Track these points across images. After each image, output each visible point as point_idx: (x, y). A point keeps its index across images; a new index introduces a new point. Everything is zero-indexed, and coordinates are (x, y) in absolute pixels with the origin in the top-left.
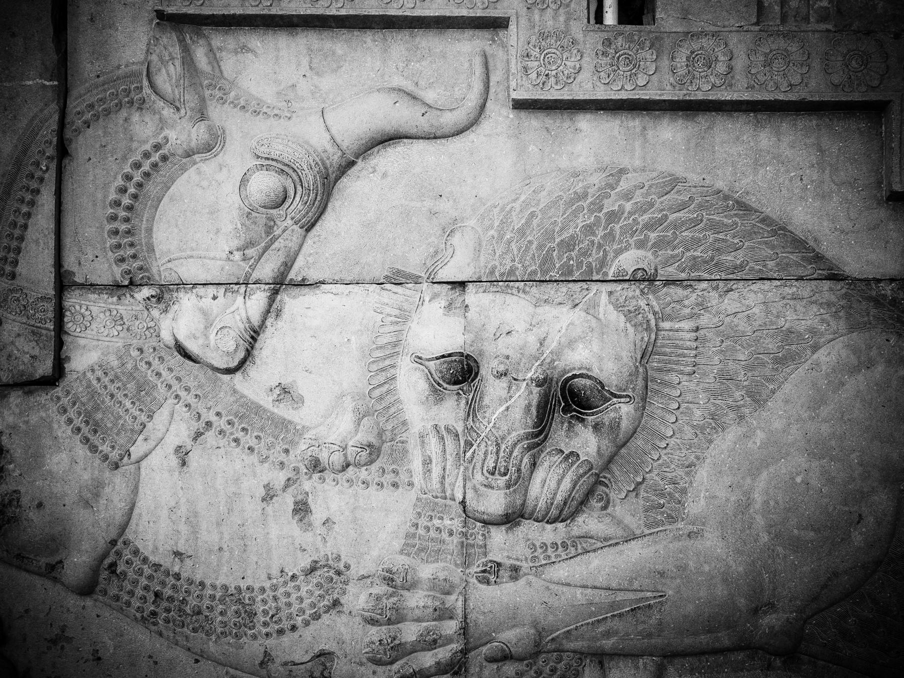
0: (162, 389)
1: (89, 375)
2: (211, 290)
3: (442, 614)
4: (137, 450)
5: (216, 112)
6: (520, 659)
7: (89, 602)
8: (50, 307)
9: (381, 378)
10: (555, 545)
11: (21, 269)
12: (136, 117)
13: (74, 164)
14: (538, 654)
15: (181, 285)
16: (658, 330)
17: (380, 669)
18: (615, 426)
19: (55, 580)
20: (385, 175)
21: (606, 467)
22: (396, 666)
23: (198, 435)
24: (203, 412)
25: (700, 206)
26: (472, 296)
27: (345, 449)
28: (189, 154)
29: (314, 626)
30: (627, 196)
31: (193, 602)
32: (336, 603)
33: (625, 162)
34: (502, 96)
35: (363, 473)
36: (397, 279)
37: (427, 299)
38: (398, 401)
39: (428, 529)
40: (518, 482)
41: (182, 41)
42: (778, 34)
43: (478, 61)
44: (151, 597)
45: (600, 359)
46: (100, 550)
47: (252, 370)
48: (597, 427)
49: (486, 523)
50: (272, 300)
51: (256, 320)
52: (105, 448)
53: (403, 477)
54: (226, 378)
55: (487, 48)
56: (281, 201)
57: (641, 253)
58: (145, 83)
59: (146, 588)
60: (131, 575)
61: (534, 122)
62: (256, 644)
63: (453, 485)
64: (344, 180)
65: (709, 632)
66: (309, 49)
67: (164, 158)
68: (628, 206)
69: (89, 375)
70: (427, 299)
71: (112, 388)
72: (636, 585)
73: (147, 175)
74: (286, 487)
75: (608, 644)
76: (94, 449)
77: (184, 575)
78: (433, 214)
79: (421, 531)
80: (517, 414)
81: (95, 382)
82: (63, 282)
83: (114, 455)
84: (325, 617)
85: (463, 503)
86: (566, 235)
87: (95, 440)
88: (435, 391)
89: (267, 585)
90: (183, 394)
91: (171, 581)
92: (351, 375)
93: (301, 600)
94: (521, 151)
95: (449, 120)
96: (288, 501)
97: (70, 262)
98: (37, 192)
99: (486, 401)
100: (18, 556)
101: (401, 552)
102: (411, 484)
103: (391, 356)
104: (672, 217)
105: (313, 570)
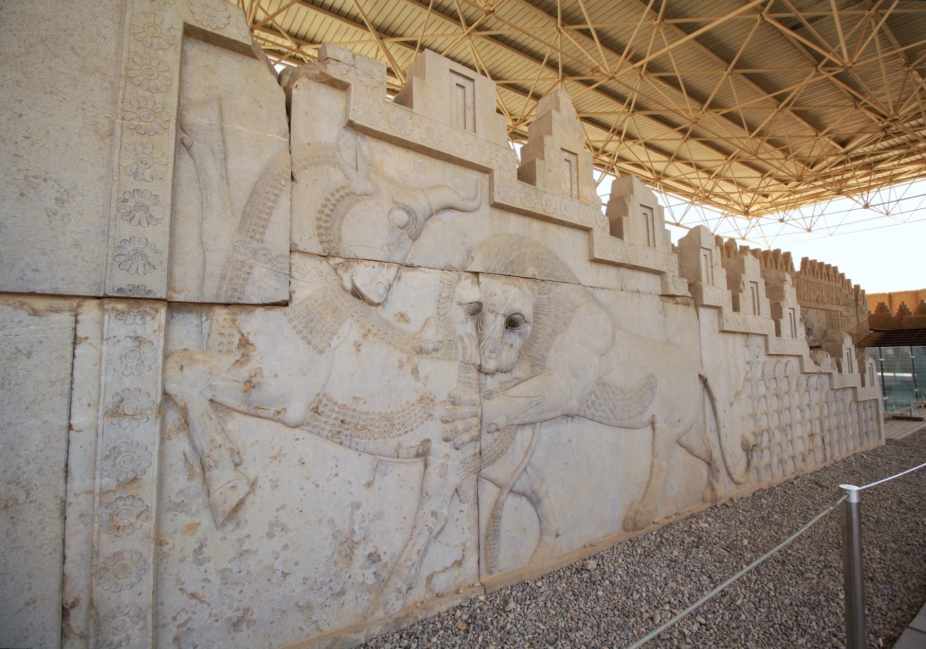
4: (334, 343)
11: (266, 238)
12: (332, 170)
15: (357, 260)
17: (447, 444)
19: (278, 421)
20: (444, 223)
23: (365, 335)
32: (431, 415)
48: (520, 335)
51: (391, 280)
59: (336, 419)
60: (327, 412)
76: (309, 343)
77: (358, 409)
81: (310, 306)
85: (480, 366)
96: (408, 368)
99: (487, 322)
105: (421, 400)
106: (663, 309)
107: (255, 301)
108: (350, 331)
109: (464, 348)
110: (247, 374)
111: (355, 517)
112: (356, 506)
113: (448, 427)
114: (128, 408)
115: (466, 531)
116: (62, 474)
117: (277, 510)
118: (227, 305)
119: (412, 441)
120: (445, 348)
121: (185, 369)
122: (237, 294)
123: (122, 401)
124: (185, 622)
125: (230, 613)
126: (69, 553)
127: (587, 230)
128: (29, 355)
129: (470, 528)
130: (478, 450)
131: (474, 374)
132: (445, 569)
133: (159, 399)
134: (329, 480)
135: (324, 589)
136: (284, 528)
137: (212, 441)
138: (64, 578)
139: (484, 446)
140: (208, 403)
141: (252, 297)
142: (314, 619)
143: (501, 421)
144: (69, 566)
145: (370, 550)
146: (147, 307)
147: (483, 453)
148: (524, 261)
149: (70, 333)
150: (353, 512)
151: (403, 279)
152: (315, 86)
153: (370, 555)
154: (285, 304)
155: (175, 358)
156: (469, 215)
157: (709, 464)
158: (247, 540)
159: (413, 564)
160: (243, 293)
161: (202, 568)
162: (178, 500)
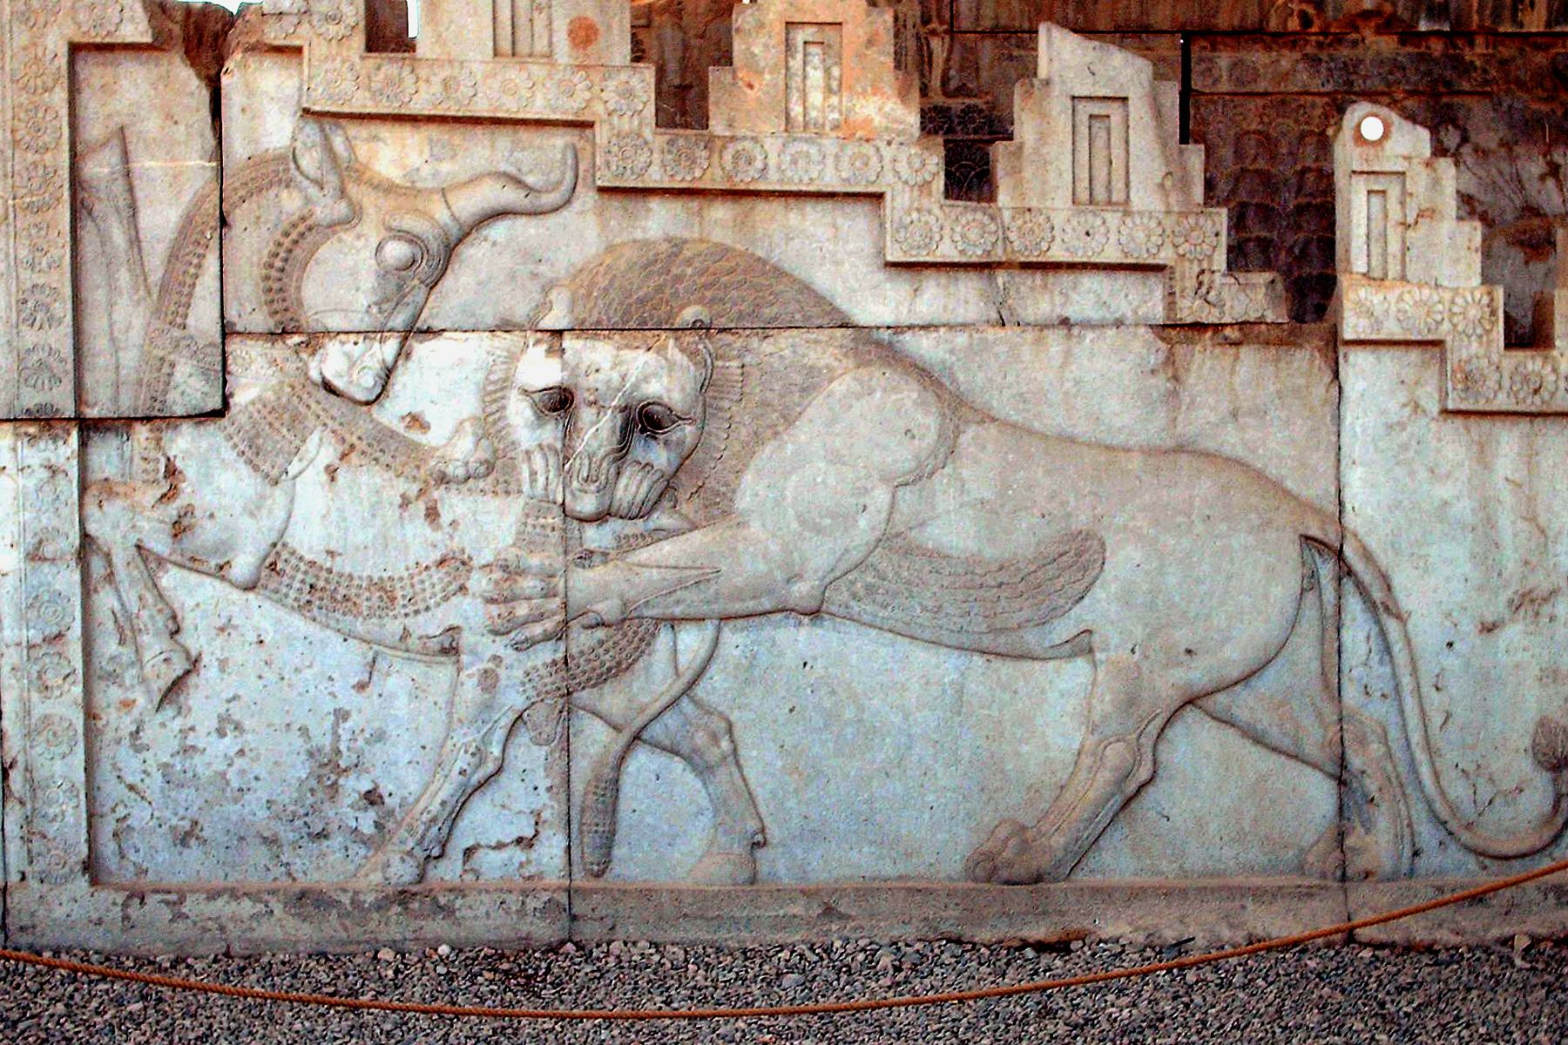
0: (312, 418)
1: (251, 408)
2: (353, 337)
3: (549, 594)
4: (293, 469)
5: (352, 189)
6: (609, 626)
7: (251, 595)
9: (494, 407)
11: (190, 321)
12: (284, 194)
13: (232, 233)
14: (624, 620)
15: (327, 333)
17: (498, 639)
18: (680, 443)
19: (223, 578)
22: (512, 635)
23: (344, 456)
24: (347, 437)
25: (745, 272)
27: (466, 464)
28: (330, 226)
29: (444, 605)
30: (689, 262)
31: (342, 591)
33: (686, 235)
34: (590, 180)
35: (481, 484)
36: (506, 327)
37: (531, 342)
38: (508, 425)
39: (534, 526)
40: (607, 488)
41: (322, 130)
42: (801, 139)
43: (570, 156)
45: (669, 391)
46: (263, 553)
47: (387, 404)
48: (666, 443)
49: (581, 520)
50: (402, 346)
51: (390, 359)
52: (266, 467)
53: (513, 487)
54: (365, 408)
55: (578, 146)
58: (292, 166)
59: (303, 581)
61: (615, 203)
62: (397, 622)
63: (555, 492)
65: (754, 597)
66: (431, 141)
68: (689, 271)
69: (251, 408)
70: (531, 342)
71: (270, 418)
72: (698, 564)
73: (296, 242)
74: (418, 498)
75: (678, 611)
76: (256, 468)
78: (535, 275)
79: (529, 529)
80: (604, 434)
82: (227, 331)
83: (274, 473)
84: (454, 600)
86: (641, 293)
87: (257, 461)
88: (538, 418)
89: (406, 574)
90: (329, 422)
91: (324, 574)
92: (469, 405)
94: (604, 226)
96: (420, 507)
97: (232, 314)
99: (580, 424)
100: (193, 559)
101: (514, 544)
102: (520, 492)
103: (502, 389)
104: (724, 279)
105: (442, 562)
106: (1170, 360)
107: (180, 411)
108: (320, 450)
109: (533, 473)
110: (175, 513)
111: (340, 731)
112: (341, 715)
113: (503, 609)
114: (48, 550)
115: (542, 790)
117: (229, 701)
118: (148, 419)
119: (430, 625)
120: (494, 469)
121: (105, 504)
122: (157, 405)
123: (40, 542)
125: (174, 821)
127: (878, 197)
130: (560, 655)
131: (555, 519)
132: (500, 846)
133: (77, 543)
135: (297, 823)
136: (238, 727)
139: (574, 651)
140: (134, 551)
141: (174, 408)
142: (284, 859)
143: (607, 608)
145: (366, 786)
148: (676, 294)
150: (336, 725)
151: (414, 356)
152: (253, 61)
153: (369, 792)
154: (219, 414)
155: (93, 491)
156: (552, 220)
157: (1341, 782)
158: (191, 734)
159: (434, 820)
161: (141, 756)
162: (110, 668)
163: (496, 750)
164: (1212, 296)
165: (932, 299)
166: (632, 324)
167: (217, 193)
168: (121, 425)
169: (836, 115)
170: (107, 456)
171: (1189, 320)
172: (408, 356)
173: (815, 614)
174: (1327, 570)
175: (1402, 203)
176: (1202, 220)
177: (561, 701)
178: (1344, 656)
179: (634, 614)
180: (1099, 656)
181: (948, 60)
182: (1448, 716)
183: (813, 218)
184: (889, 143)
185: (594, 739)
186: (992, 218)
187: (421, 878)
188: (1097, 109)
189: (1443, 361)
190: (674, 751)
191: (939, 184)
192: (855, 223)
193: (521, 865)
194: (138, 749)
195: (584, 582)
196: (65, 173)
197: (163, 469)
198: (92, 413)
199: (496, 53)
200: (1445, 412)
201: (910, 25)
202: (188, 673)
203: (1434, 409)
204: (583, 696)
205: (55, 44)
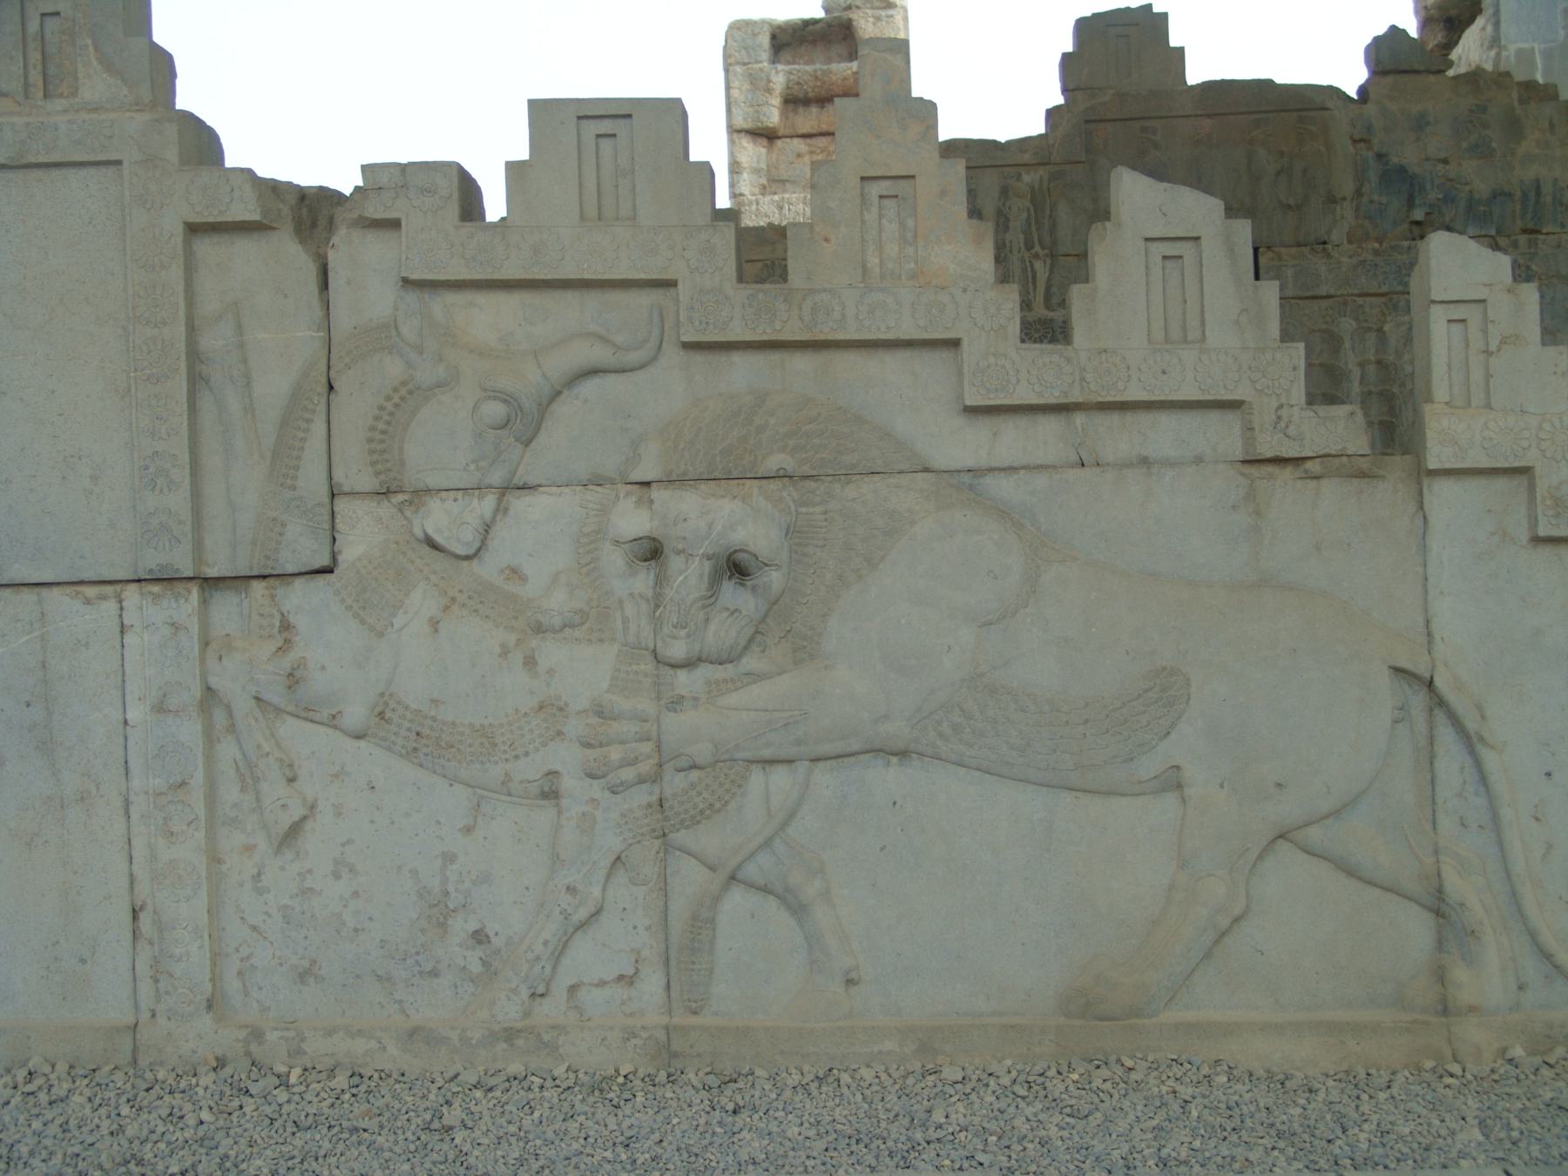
2: (452, 494)
4: (399, 621)
7: (362, 743)
8: (325, 511)
10: (725, 681)
15: (428, 491)
16: (798, 513)
17: (595, 782)
19: (335, 727)
20: (586, 401)
21: (763, 620)
23: (446, 608)
26: (656, 493)
32: (559, 733)
35: (577, 633)
36: (597, 481)
44: (413, 736)
48: (754, 589)
50: (500, 500)
51: (488, 514)
54: (465, 563)
56: (505, 425)
57: (782, 456)
58: (394, 333)
59: (409, 730)
61: (699, 358)
64: (554, 405)
67: (411, 392)
74: (517, 645)
75: (767, 753)
76: (363, 622)
93: (531, 731)
95: (634, 357)
97: (339, 475)
98: (308, 421)
100: (307, 709)
105: (541, 708)
107: (290, 569)
108: (422, 602)
109: (625, 621)
111: (448, 873)
112: (448, 858)
116: (122, 770)
118: (264, 577)
119: (530, 770)
121: (224, 659)
124: (248, 958)
126: (135, 854)
127: (955, 344)
128: (87, 645)
129: (648, 928)
130: (655, 798)
131: (647, 666)
132: (602, 984)
134: (408, 815)
137: (259, 747)
138: (132, 880)
139: (668, 792)
140: (253, 701)
144: (135, 867)
145: (473, 925)
146: (180, 587)
147: (666, 805)
149: (117, 620)
153: (476, 932)
154: (328, 570)
157: (1438, 913)
159: (538, 958)
160: (276, 560)
163: (596, 892)
164: (1292, 430)
165: (1013, 441)
166: (716, 474)
167: (324, 361)
168: (238, 581)
169: (912, 265)
170: (227, 610)
171: (1269, 455)
172: (506, 510)
173: (903, 754)
174: (1418, 700)
175: (1485, 331)
176: (1278, 356)
177: (657, 843)
178: (1438, 789)
179: (726, 757)
180: (1188, 791)
181: (1049, 280)
182: (1550, 847)
183: (891, 366)
184: (965, 291)
185: (690, 878)
186: (1068, 360)
187: (527, 1014)
188: (1169, 248)
189: (1532, 487)
190: (765, 890)
191: (1015, 328)
192: (932, 365)
193: (623, 1003)
194: (260, 891)
195: (677, 725)
196: (182, 346)
197: (278, 624)
198: (212, 572)
199: (583, 218)
200: (1537, 540)
201: (1015, 251)
202: (304, 818)
203: (1524, 537)
204: (680, 837)
205: (171, 226)
